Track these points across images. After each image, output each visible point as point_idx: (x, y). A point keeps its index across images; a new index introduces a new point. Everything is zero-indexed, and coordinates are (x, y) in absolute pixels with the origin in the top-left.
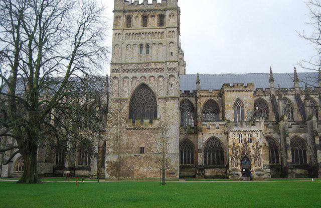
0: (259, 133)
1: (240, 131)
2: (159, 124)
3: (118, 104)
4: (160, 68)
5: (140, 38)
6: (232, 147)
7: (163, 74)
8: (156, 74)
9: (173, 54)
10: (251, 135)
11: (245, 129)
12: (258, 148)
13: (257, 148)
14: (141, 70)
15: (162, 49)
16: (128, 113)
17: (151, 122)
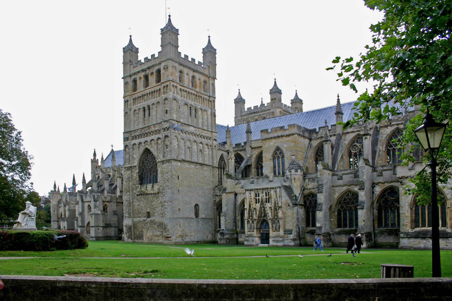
0: (278, 190)
1: (257, 189)
2: (159, 189)
3: (129, 172)
4: (158, 130)
5: (143, 101)
6: (248, 209)
7: (160, 136)
8: (155, 137)
9: (168, 112)
10: (269, 193)
11: (261, 187)
12: (276, 208)
13: (276, 209)
14: (147, 134)
15: (161, 108)
16: (138, 179)
17: (153, 187)
